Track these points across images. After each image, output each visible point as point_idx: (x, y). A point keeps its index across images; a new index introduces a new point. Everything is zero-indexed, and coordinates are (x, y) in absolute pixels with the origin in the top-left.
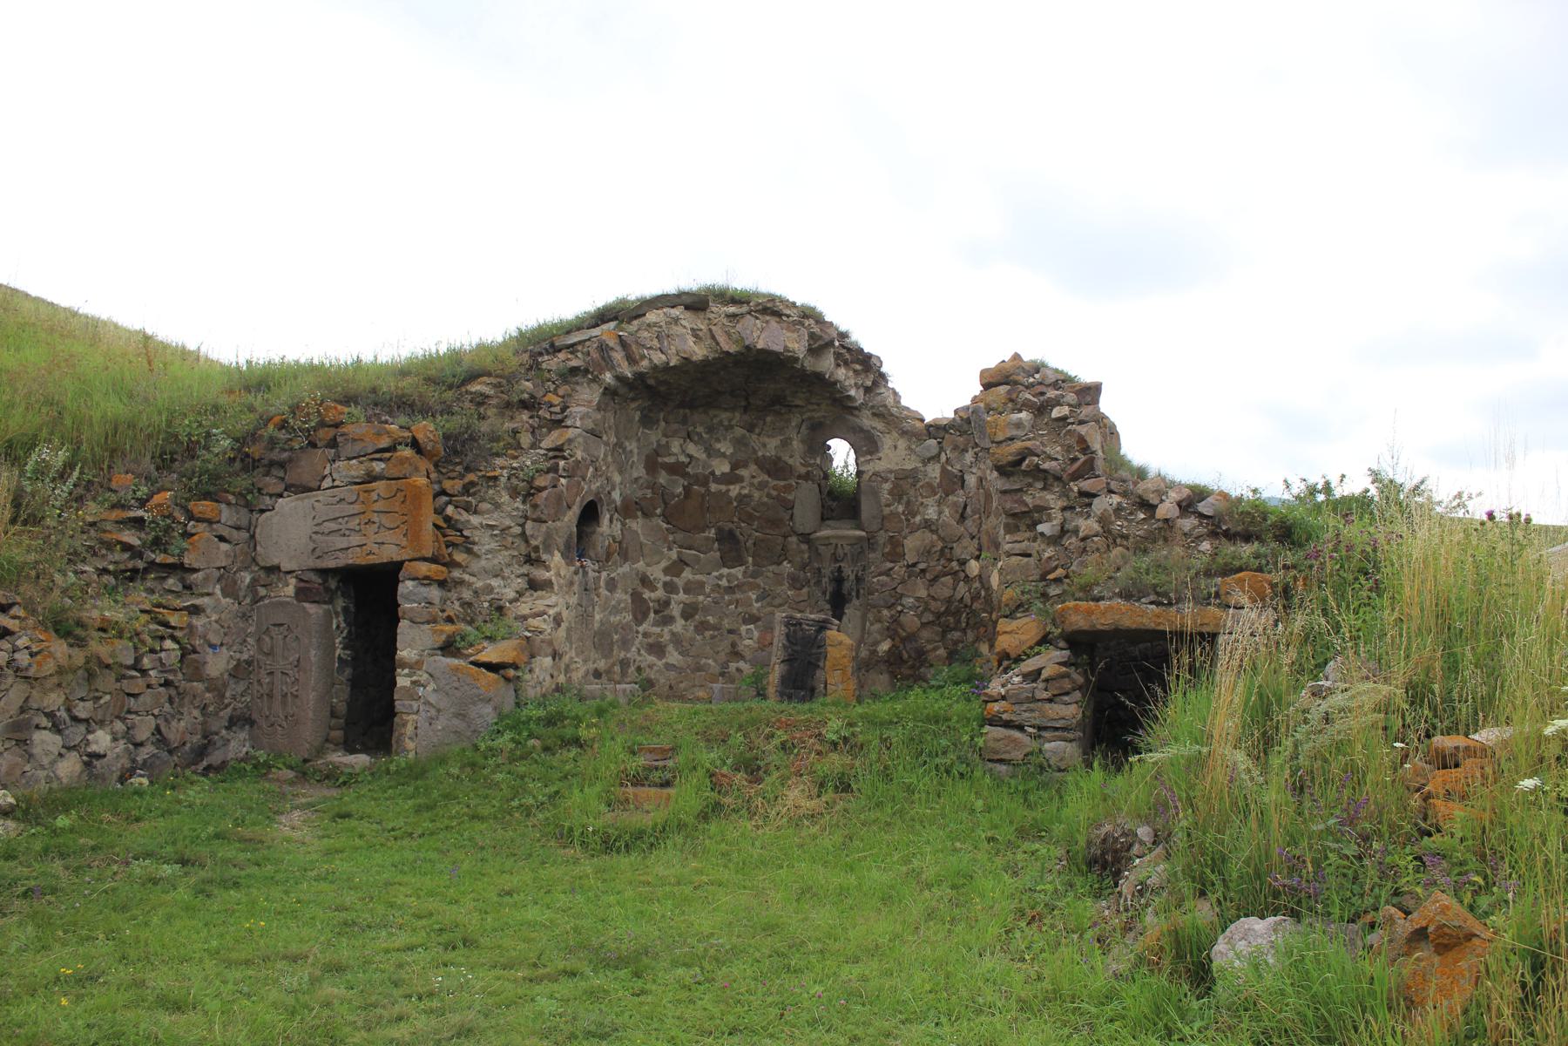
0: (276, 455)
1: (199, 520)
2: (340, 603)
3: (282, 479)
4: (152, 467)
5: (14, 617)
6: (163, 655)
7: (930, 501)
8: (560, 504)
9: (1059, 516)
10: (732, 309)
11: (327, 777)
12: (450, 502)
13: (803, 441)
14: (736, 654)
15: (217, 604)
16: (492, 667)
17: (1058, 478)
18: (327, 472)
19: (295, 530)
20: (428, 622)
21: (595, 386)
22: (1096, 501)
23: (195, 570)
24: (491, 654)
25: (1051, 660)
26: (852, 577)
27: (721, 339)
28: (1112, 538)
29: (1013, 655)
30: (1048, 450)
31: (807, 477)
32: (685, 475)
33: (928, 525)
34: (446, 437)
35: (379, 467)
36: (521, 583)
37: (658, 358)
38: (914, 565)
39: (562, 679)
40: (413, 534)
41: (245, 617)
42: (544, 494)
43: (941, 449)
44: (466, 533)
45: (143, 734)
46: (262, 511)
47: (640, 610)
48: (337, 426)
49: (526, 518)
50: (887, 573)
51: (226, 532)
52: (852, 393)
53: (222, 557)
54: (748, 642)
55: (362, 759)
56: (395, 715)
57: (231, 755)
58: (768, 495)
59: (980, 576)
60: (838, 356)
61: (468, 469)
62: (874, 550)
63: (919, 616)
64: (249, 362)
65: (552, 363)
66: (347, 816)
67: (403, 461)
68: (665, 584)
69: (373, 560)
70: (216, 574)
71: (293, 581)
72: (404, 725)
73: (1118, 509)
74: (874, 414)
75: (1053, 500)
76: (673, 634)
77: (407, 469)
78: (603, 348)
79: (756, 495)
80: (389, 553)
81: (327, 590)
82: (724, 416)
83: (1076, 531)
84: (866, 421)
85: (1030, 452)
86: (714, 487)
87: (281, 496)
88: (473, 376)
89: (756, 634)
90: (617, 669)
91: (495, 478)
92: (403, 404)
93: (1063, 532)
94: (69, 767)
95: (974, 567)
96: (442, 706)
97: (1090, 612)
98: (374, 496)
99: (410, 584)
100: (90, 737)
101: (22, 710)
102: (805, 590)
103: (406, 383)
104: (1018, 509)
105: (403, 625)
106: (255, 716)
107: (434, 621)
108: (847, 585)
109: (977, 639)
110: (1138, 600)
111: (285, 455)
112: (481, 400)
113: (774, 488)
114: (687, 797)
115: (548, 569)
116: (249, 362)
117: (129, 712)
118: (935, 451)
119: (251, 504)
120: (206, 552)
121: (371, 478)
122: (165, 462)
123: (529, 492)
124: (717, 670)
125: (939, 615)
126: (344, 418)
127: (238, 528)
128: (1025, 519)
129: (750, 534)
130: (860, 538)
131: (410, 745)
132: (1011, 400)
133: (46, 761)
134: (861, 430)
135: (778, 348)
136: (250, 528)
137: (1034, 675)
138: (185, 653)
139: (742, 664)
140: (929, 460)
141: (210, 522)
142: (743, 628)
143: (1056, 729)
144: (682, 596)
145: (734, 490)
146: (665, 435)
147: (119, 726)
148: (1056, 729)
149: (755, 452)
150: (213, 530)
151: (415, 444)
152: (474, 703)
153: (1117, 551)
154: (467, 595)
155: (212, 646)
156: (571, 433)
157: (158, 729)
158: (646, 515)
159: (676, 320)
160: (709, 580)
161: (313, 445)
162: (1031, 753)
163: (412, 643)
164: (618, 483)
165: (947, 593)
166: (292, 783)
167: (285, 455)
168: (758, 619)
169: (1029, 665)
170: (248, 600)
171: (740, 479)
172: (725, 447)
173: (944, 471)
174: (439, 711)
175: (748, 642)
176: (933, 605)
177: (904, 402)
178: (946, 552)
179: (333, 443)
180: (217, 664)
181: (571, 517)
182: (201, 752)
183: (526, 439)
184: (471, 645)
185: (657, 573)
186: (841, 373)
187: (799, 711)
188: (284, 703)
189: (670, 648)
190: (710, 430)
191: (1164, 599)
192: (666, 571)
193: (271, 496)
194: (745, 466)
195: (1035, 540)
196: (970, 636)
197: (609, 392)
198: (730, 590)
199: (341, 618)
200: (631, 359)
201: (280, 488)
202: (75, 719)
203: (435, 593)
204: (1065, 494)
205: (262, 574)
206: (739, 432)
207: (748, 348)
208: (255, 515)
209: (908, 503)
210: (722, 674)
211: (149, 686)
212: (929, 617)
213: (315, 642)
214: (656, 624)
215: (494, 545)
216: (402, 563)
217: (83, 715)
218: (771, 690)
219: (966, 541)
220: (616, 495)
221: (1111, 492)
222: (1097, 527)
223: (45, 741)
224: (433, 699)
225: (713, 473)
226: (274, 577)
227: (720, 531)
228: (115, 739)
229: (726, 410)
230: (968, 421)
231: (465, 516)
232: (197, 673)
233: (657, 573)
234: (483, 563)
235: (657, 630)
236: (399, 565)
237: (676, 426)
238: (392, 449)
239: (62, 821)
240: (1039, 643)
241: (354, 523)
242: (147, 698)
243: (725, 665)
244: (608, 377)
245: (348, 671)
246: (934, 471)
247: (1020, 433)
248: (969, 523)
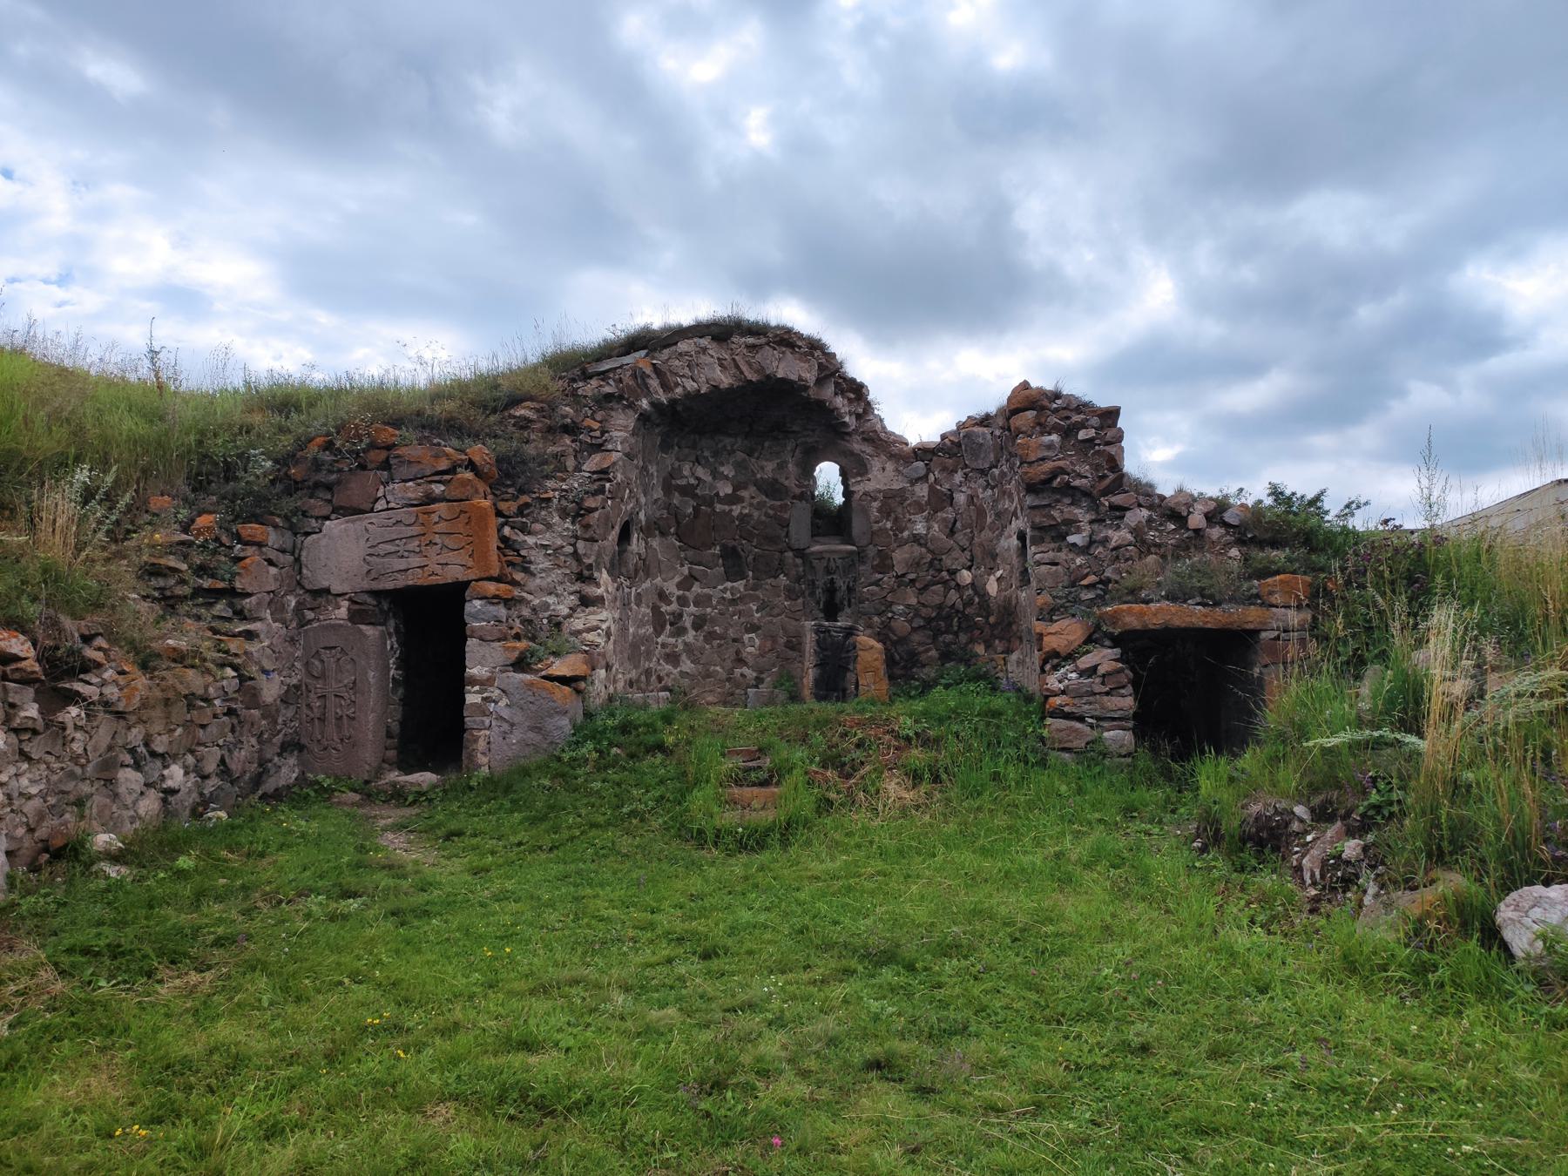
0: (322, 477)
1: (246, 544)
2: (392, 623)
3: (330, 501)
4: (187, 490)
5: (100, 649)
6: (225, 683)
7: (918, 518)
8: (607, 523)
9: (1088, 527)
10: (751, 340)
11: (392, 797)
12: (506, 523)
13: (797, 465)
14: (740, 661)
15: (268, 626)
16: (564, 680)
17: (1086, 494)
19: (343, 552)
20: (499, 640)
21: (630, 412)
22: (1128, 514)
23: (249, 595)
24: (560, 667)
25: (1104, 658)
26: (844, 588)
27: (744, 368)
28: (1144, 546)
29: (1063, 654)
30: (1077, 468)
31: (801, 497)
32: (695, 496)
33: (916, 539)
34: (499, 460)
35: (438, 489)
36: (573, 600)
37: (691, 385)
38: (903, 575)
39: (611, 689)
40: (478, 555)
41: (292, 641)
42: (596, 514)
43: (929, 470)
44: (523, 553)
45: (211, 766)
46: (307, 534)
47: (659, 622)
48: (389, 447)
49: (577, 538)
50: (877, 583)
51: (273, 555)
52: (847, 419)
53: (271, 580)
54: (749, 649)
55: (426, 778)
56: (465, 731)
57: (282, 783)
58: (766, 515)
59: (972, 584)
60: (837, 384)
61: (522, 491)
62: (864, 563)
63: (910, 622)
64: (247, 384)
65: (590, 388)
66: (459, 834)
67: (467, 482)
68: (679, 598)
69: (434, 580)
70: (267, 598)
72: (476, 740)
73: (1150, 520)
74: (864, 439)
75: (1082, 514)
76: (686, 644)
77: (469, 491)
78: (638, 375)
79: (756, 514)
81: (382, 611)
82: (728, 441)
83: (1106, 540)
84: (857, 446)
85: (1062, 471)
86: (719, 507)
87: (327, 518)
88: (515, 401)
90: (643, 678)
91: (549, 500)
92: (452, 427)
93: (1091, 542)
94: (149, 805)
95: (966, 576)
96: (516, 720)
97: (1142, 614)
99: (477, 603)
100: (166, 772)
101: (110, 748)
102: (800, 600)
103: (450, 406)
104: (1046, 522)
105: (471, 643)
106: (304, 741)
107: (505, 639)
108: (839, 595)
109: (972, 641)
110: (1185, 601)
111: (334, 477)
112: (524, 424)
113: (772, 507)
114: (793, 796)
115: (598, 585)
116: (247, 384)
117: (199, 744)
118: (923, 472)
119: (297, 527)
120: (259, 577)
121: (430, 499)
122: (199, 484)
123: (579, 513)
124: (724, 676)
125: (929, 620)
126: (396, 440)
127: (283, 551)
128: (1056, 533)
129: (750, 550)
130: (851, 552)
131: (483, 760)
132: (1039, 424)
133: (129, 801)
134: (852, 453)
135: (794, 377)
136: (294, 551)
137: (1092, 671)
138: (242, 678)
139: (745, 670)
140: (918, 480)
141: (260, 545)
142: (746, 636)
143: (1114, 719)
144: (692, 609)
145: (736, 510)
146: (678, 459)
147: (190, 759)
148: (1114, 719)
149: (754, 474)
150: (262, 553)
151: (471, 465)
152: (551, 716)
153: (1151, 559)
154: (526, 612)
155: (265, 672)
156: (615, 456)
157: (223, 761)
158: (663, 534)
159: (704, 350)
160: (716, 593)
161: (363, 467)
162: (1093, 742)
163: (481, 660)
164: (643, 505)
165: (937, 600)
166: (359, 805)
167: (334, 477)
168: (759, 628)
169: (1085, 662)
170: (294, 624)
171: (740, 500)
172: (727, 470)
173: (931, 488)
174: (512, 725)
175: (749, 649)
176: (924, 611)
177: (890, 428)
178: (935, 564)
179: (386, 465)
180: (270, 690)
181: (614, 535)
182: (257, 781)
183: (570, 463)
184: (540, 661)
185: (671, 588)
186: (839, 401)
187: (829, 708)
188: (339, 727)
189: (684, 657)
190: (716, 454)
191: (1210, 599)
192: (679, 586)
193: (317, 518)
194: (745, 488)
195: (1060, 550)
196: (963, 638)
197: (644, 418)
198: (733, 602)
200: (666, 387)
201: (326, 510)
202: (153, 754)
203: (502, 611)
204: (1095, 506)
205: (308, 598)
206: (740, 455)
207: (768, 377)
208: (300, 538)
209: (896, 520)
210: (729, 680)
211: (215, 716)
212: (919, 622)
213: (371, 665)
214: (672, 635)
215: (547, 564)
217: (160, 750)
218: (807, 692)
219: (957, 553)
220: (642, 516)
221: (1140, 505)
222: (1130, 537)
223: (129, 778)
224: (505, 714)
225: (717, 494)
227: (724, 548)
228: (186, 773)
229: (730, 435)
230: (959, 445)
231: (521, 537)
232: (253, 699)
233: (671, 588)
234: (538, 581)
235: (672, 640)
236: (466, 584)
237: (686, 451)
238: (452, 470)
239: (184, 862)
240: (1086, 642)
242: (213, 729)
244: (644, 403)
245: (401, 691)
246: (922, 491)
247: (1050, 454)
248: (959, 536)
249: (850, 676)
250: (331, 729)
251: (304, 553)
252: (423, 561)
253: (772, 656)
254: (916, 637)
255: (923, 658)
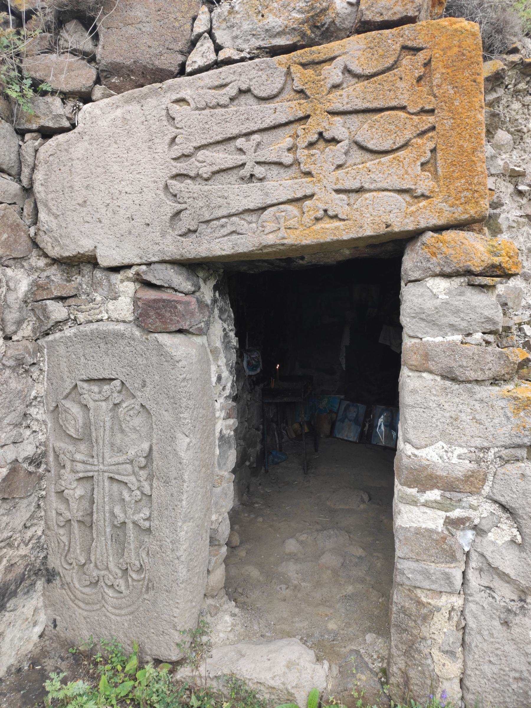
18: (200, 27)
46: (46, 133)
69: (329, 232)
71: (127, 288)
80: (399, 216)
81: (201, 303)
87: (86, 98)
98: (333, 73)
99: (440, 286)
105: (412, 384)
106: (54, 562)
170: (27, 330)
193: (65, 96)
199: (222, 361)
201: (83, 76)
205: (55, 274)
208: (31, 142)
216: (413, 236)
224: (509, 562)
226: (81, 280)
241: (277, 146)
250: (103, 547)
251: (39, 176)
252: (304, 187)
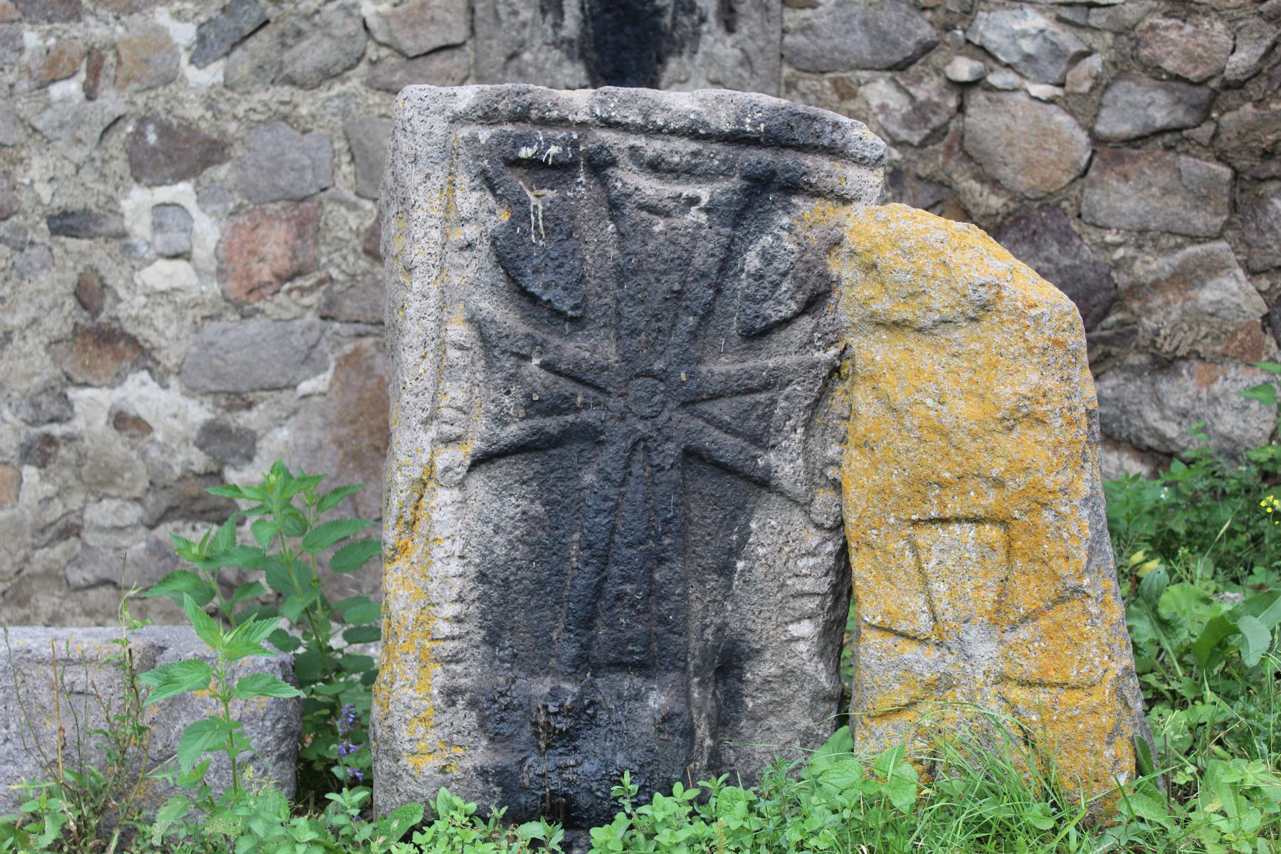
14: (104, 340)
54: (160, 274)
63: (1084, 107)
89: (208, 231)
139: (138, 392)
142: (138, 202)
175: (160, 274)
210: (40, 451)
212: (1141, 106)
243: (52, 402)
249: (781, 546)
253: (295, 309)
254: (1124, 198)
255: (1161, 318)
